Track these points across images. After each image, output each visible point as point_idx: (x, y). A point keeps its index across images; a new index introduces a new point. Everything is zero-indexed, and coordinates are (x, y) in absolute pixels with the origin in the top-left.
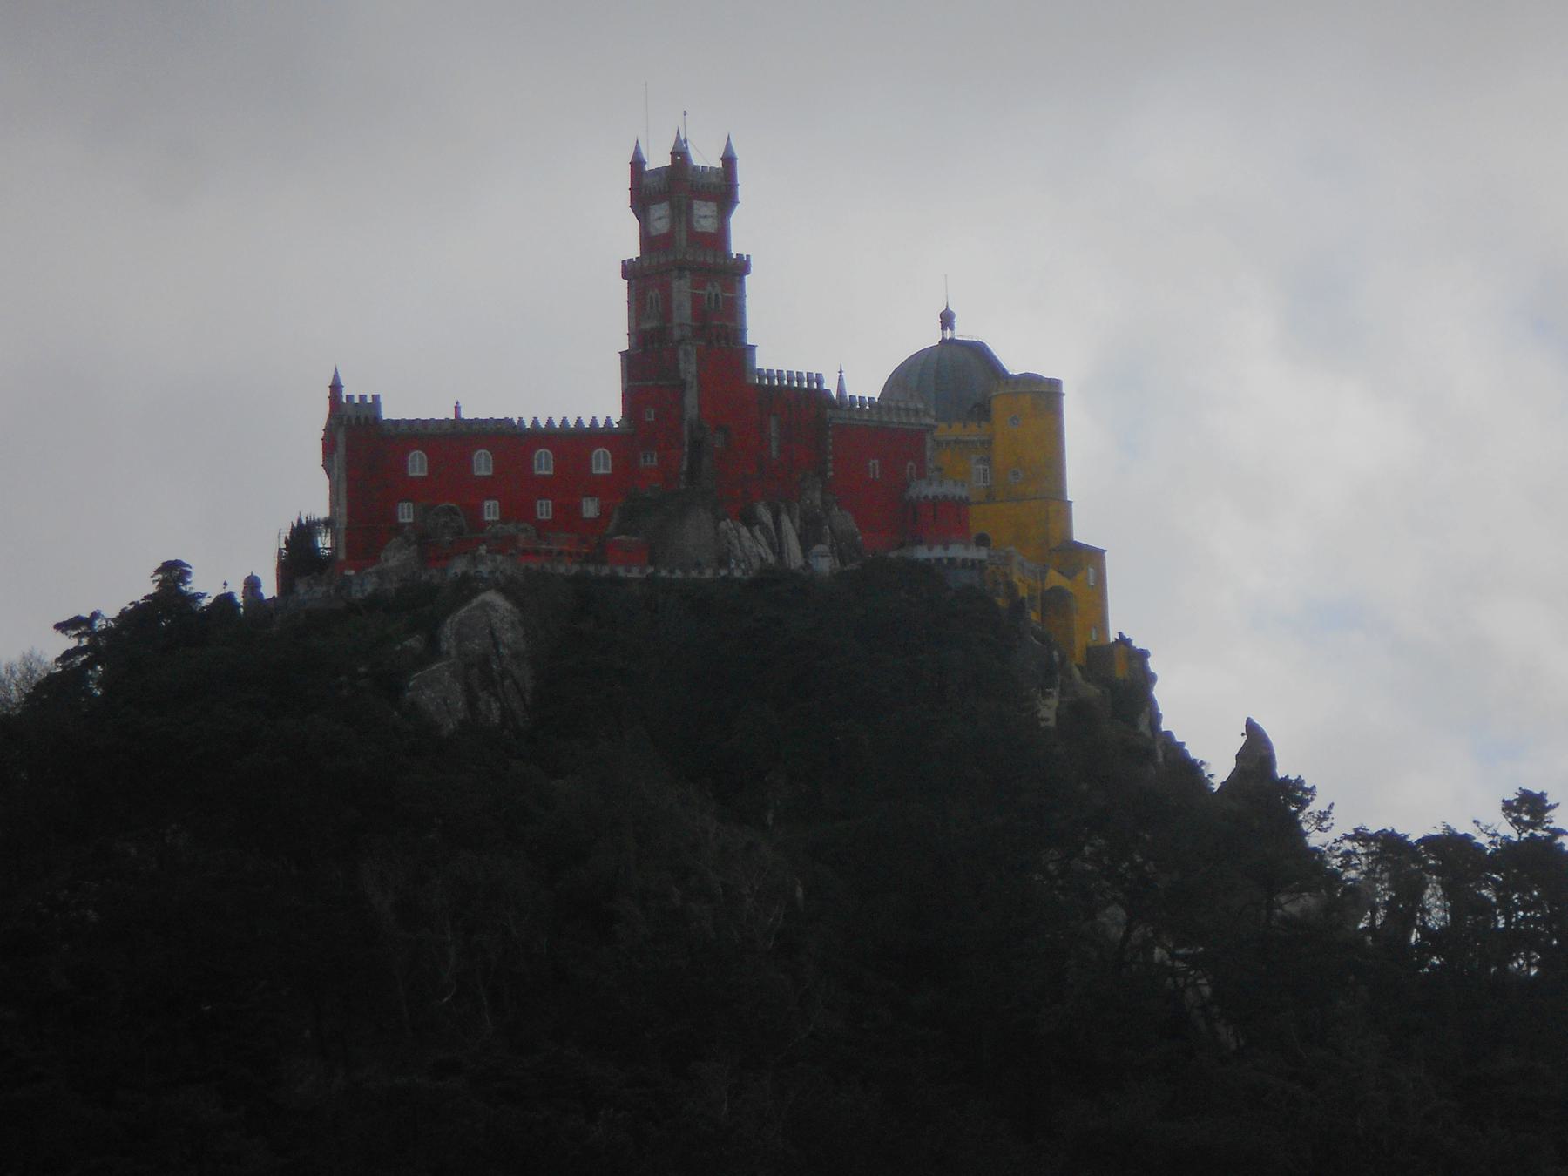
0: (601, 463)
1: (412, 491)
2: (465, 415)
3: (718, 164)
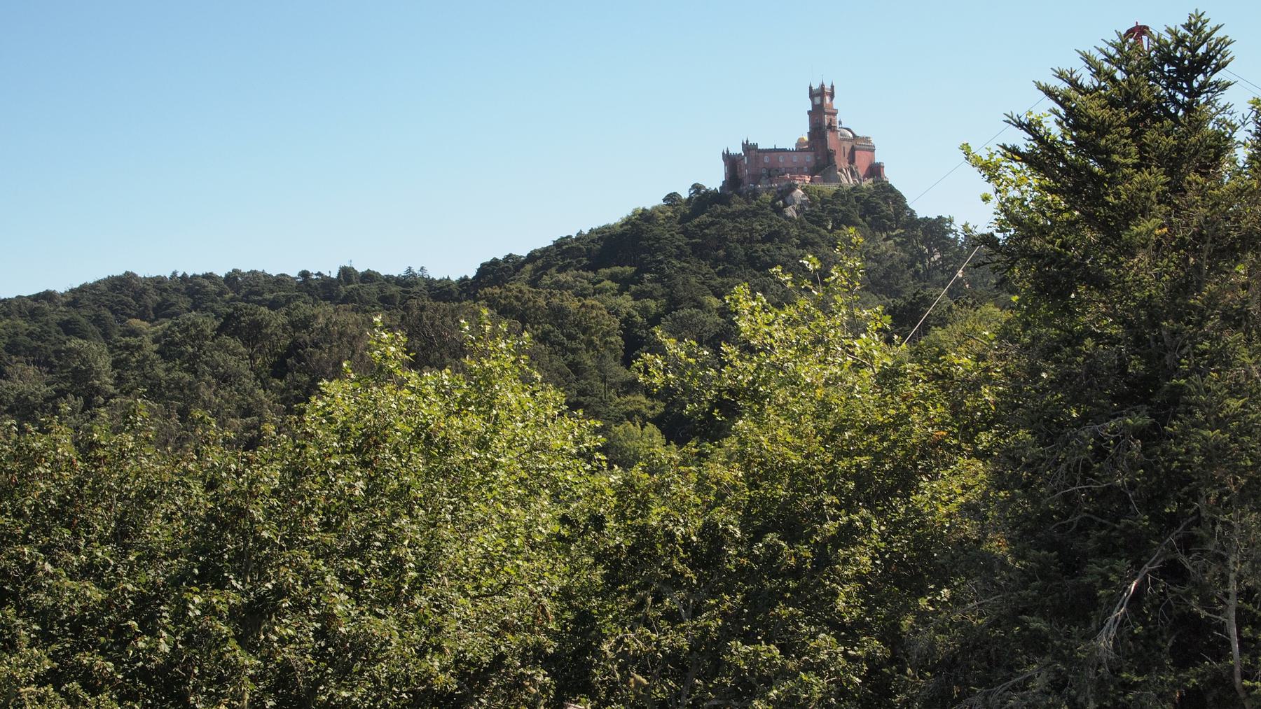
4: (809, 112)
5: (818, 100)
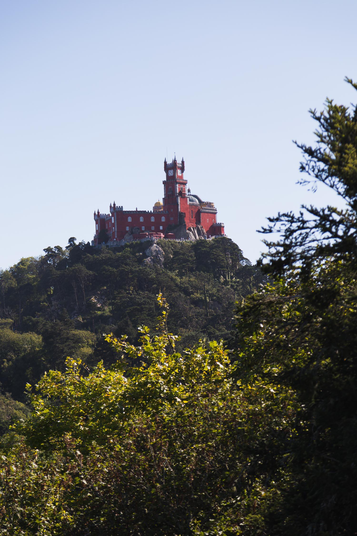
0: (163, 219)
1: (129, 224)
2: (138, 210)
3: (181, 163)
4: (164, 182)
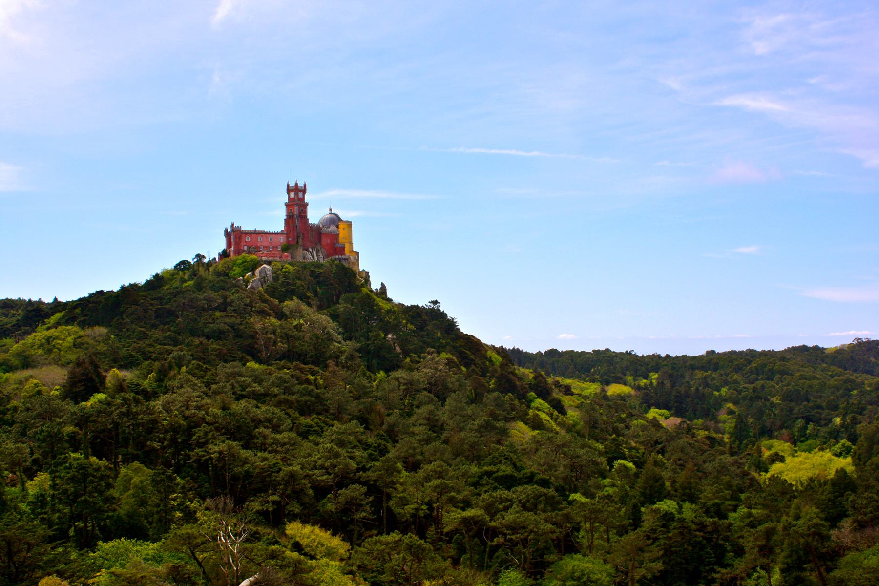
5: (292, 195)
